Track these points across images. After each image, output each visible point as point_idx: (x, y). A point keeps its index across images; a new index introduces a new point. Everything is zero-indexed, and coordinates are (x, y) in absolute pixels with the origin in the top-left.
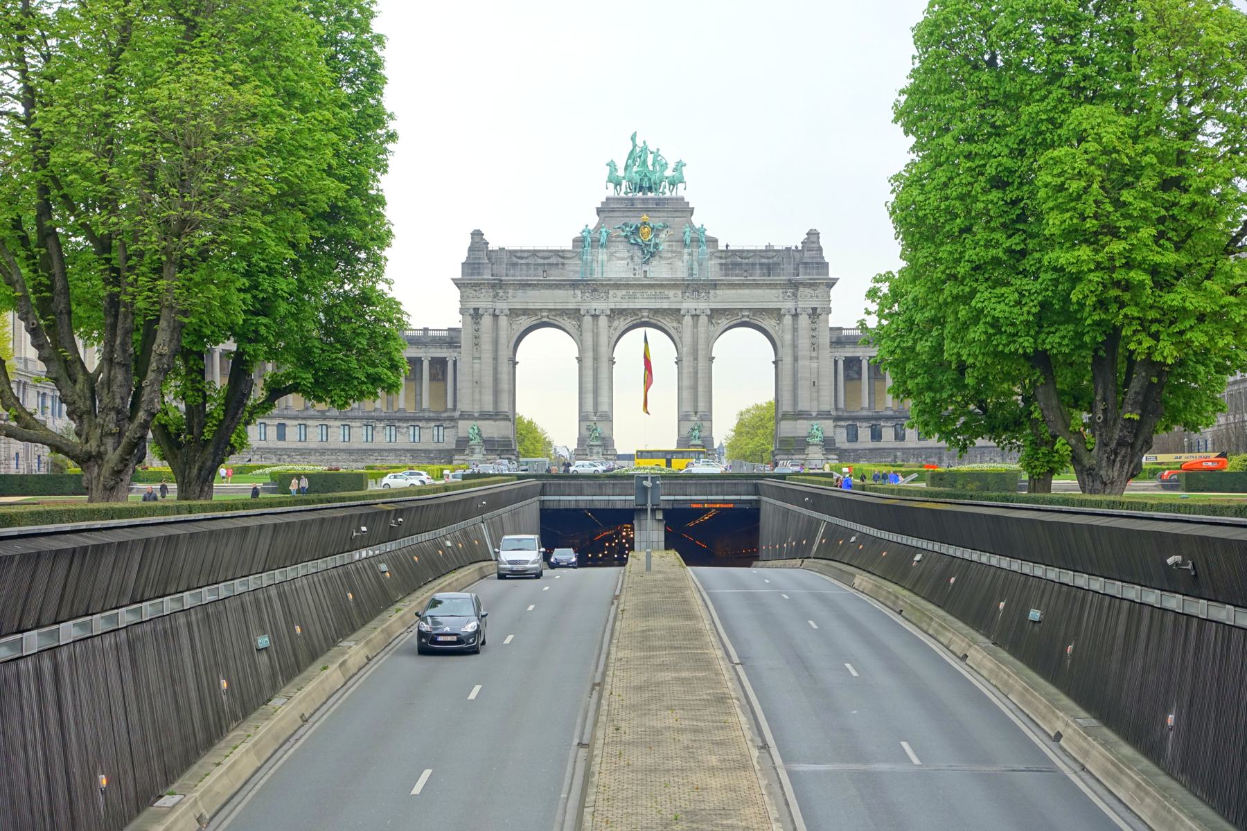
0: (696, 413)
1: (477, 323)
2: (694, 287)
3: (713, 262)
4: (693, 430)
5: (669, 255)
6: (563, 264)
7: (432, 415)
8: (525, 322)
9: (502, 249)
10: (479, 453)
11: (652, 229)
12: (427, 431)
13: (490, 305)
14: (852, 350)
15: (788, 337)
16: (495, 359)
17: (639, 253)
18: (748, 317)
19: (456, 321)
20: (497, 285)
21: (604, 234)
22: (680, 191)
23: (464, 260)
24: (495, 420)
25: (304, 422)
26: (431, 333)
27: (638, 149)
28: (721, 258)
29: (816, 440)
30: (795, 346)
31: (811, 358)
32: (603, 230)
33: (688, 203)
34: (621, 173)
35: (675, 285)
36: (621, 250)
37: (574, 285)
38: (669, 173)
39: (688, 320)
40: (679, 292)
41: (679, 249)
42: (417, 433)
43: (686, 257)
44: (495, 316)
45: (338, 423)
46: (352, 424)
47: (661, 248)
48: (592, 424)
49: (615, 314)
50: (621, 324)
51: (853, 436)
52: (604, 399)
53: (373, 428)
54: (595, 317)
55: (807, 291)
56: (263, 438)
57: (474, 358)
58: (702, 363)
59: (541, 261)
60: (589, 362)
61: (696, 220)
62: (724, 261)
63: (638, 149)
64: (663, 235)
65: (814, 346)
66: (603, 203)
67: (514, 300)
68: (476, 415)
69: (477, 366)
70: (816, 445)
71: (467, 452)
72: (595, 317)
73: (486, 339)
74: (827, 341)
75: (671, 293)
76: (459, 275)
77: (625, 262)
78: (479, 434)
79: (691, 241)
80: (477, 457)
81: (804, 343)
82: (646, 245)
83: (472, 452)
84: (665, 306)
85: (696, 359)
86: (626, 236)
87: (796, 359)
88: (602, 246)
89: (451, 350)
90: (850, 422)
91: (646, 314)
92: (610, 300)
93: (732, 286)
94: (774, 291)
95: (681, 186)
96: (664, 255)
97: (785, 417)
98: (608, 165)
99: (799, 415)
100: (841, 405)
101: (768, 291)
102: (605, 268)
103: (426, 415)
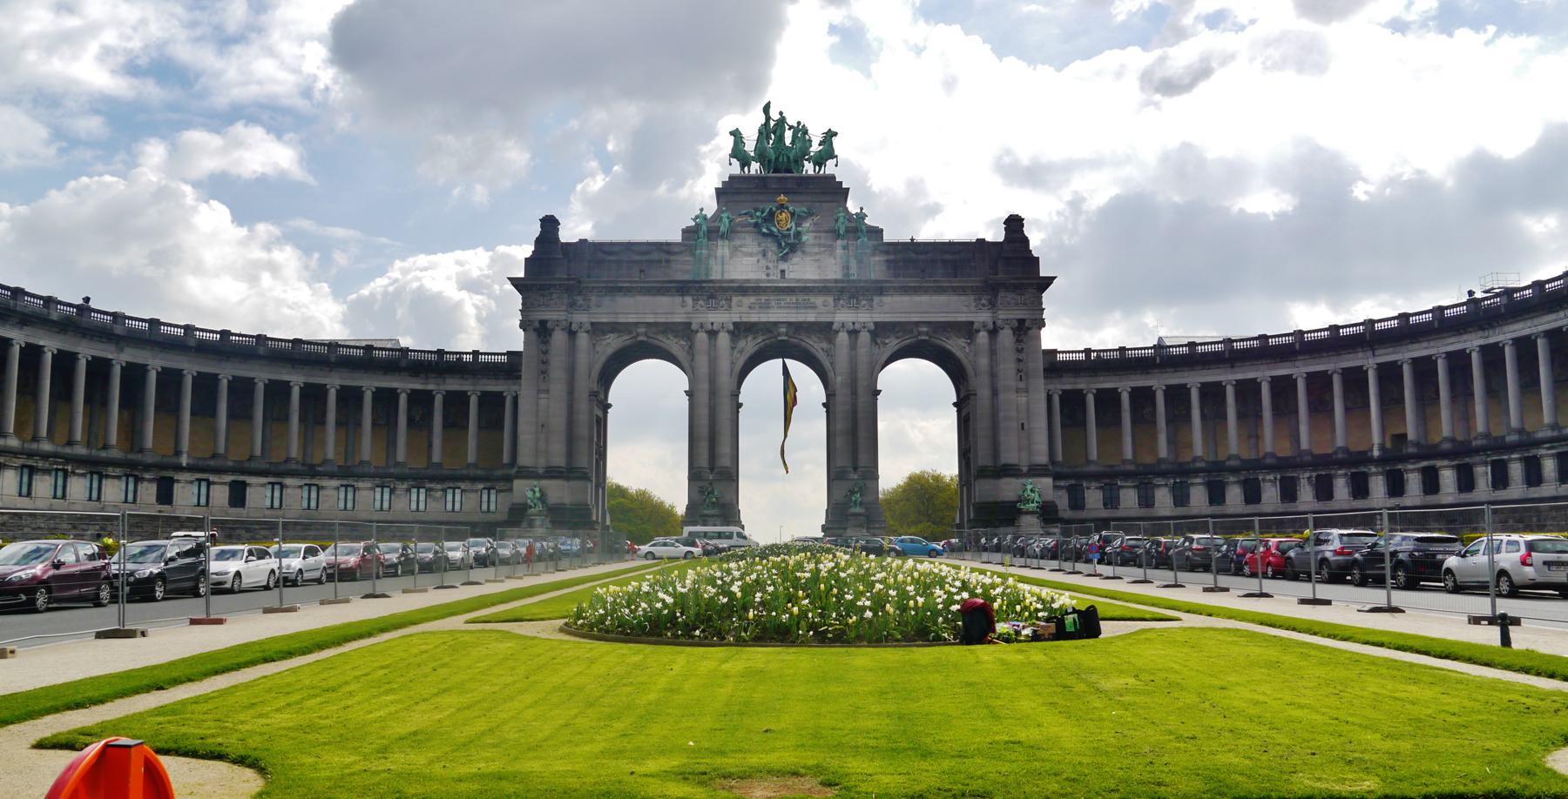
0: (855, 469)
1: (546, 342)
2: (846, 291)
3: (877, 258)
4: (852, 492)
5: (816, 250)
6: (668, 261)
7: (479, 472)
8: (613, 343)
10: (542, 526)
11: (793, 214)
12: (472, 496)
14: (1072, 380)
15: (984, 361)
16: (571, 392)
17: (772, 247)
18: (927, 334)
19: (516, 340)
20: (574, 290)
21: (726, 221)
22: (830, 168)
23: (529, 254)
24: (568, 479)
25: (279, 480)
26: (482, 358)
27: (772, 123)
28: (887, 253)
29: (1032, 506)
30: (993, 375)
31: (1018, 390)
32: (724, 215)
33: (841, 182)
34: (750, 147)
35: (823, 289)
36: (750, 243)
37: (683, 288)
38: (815, 147)
39: (843, 337)
40: (830, 300)
41: (829, 243)
42: (458, 498)
43: (839, 251)
44: (572, 334)
45: (335, 483)
46: (360, 485)
47: (804, 238)
48: (706, 484)
49: (740, 330)
50: (749, 345)
51: (1077, 503)
52: (724, 448)
53: (392, 491)
54: (712, 334)
55: (1010, 296)
56: (59, 493)
57: (539, 391)
58: (863, 399)
59: (638, 258)
60: (703, 398)
61: (852, 206)
62: (892, 257)
63: (772, 123)
64: (807, 225)
65: (1022, 374)
68: (541, 471)
69: (543, 402)
70: (1032, 513)
71: (524, 524)
72: (712, 334)
74: (1040, 365)
75: (818, 300)
76: (521, 274)
77: (755, 259)
78: (543, 498)
79: (848, 231)
80: (540, 531)
81: (1007, 368)
82: (785, 236)
83: (531, 525)
84: (811, 317)
85: (854, 393)
86: (756, 225)
87: (995, 393)
88: (722, 237)
89: (510, 382)
90: (1073, 482)
91: (783, 330)
92: (735, 309)
93: (905, 290)
94: (963, 298)
95: (830, 163)
96: (807, 250)
97: (984, 473)
98: (731, 133)
99: (1010, 471)
100: (1060, 458)
101: (954, 298)
102: (726, 267)
103: (472, 472)
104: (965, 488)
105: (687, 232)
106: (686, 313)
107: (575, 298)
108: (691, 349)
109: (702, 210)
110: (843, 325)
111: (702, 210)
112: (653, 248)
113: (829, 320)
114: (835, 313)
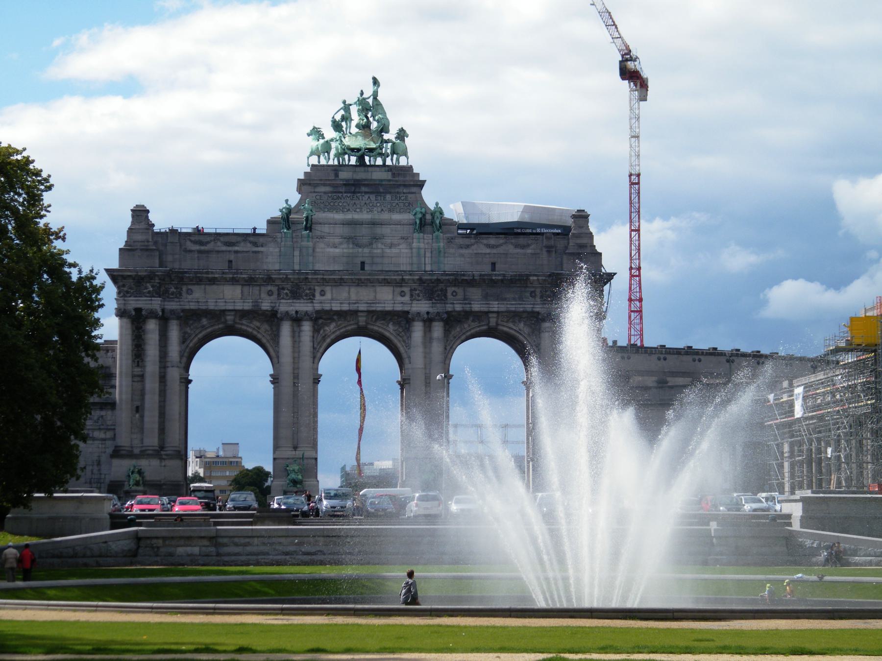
9: (173, 231)
13: (156, 304)
23: (122, 245)
33: (418, 174)
40: (407, 290)
61: (430, 197)
66: (306, 173)
67: (190, 297)
68: (137, 451)
73: (152, 351)
104: (531, 463)
105: (271, 222)
106: (271, 303)
107: (167, 286)
108: (276, 337)
109: (287, 201)
110: (419, 314)
111: (287, 201)
112: (239, 239)
113: (406, 309)
114: (411, 304)
